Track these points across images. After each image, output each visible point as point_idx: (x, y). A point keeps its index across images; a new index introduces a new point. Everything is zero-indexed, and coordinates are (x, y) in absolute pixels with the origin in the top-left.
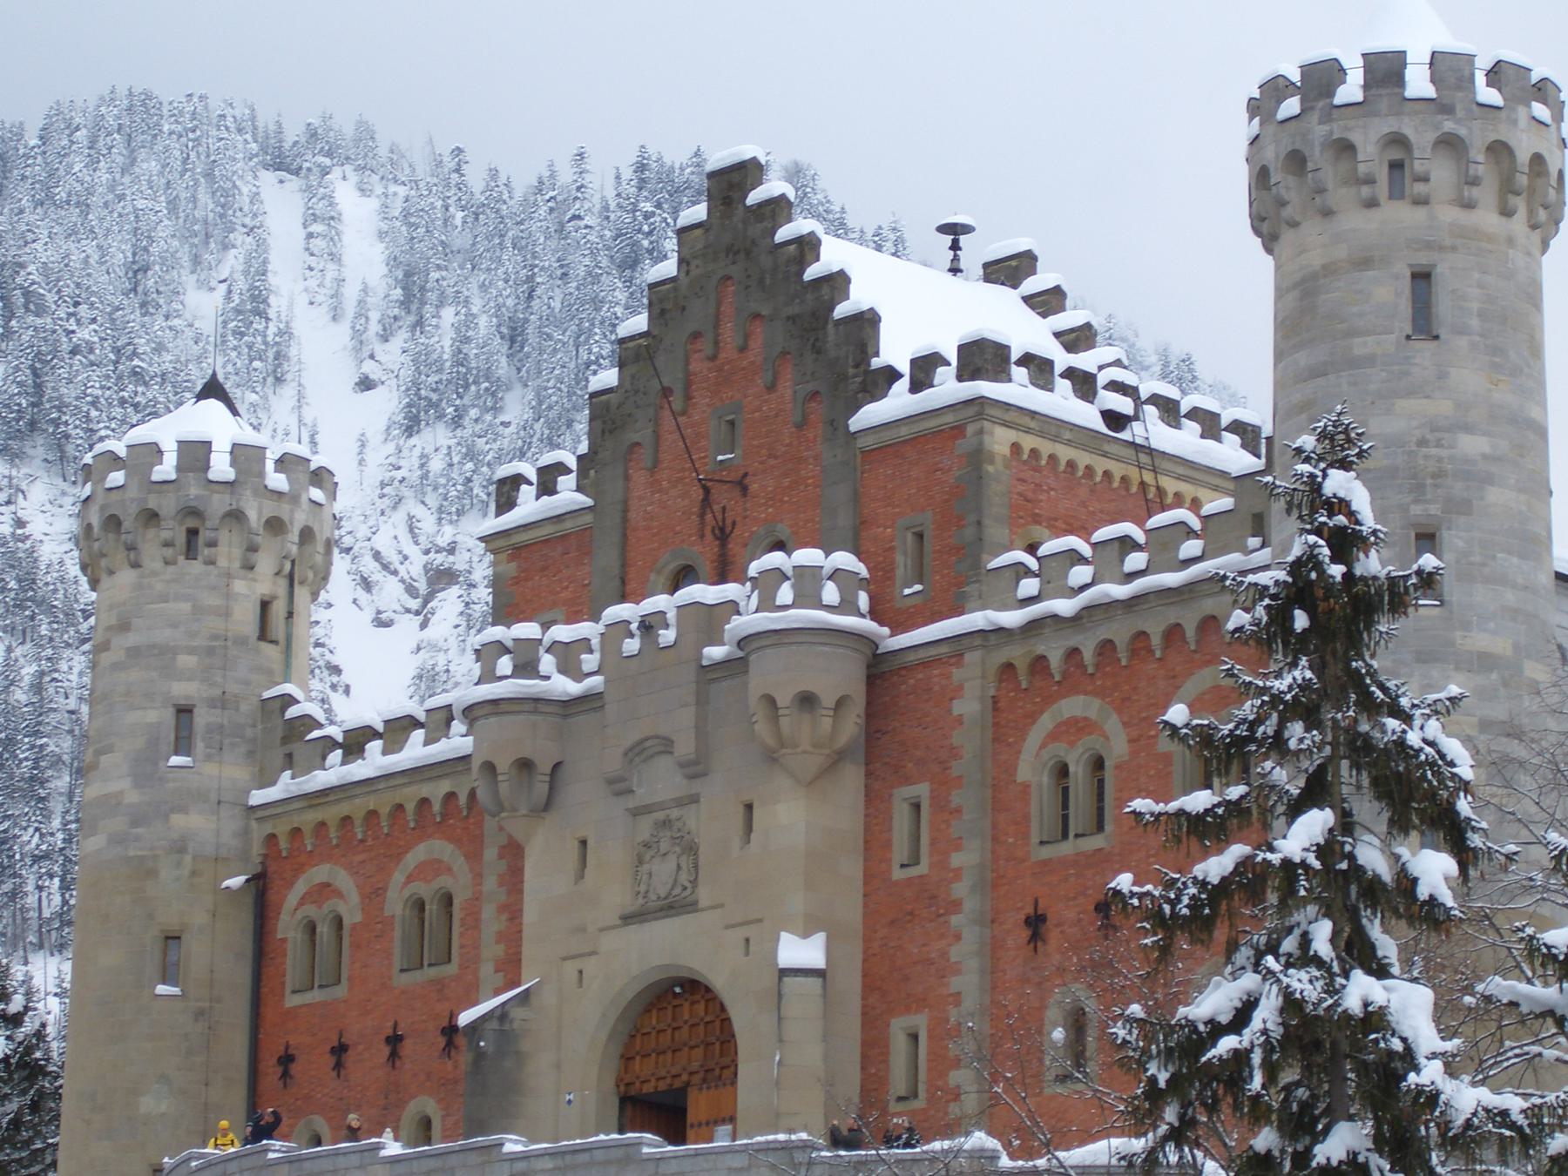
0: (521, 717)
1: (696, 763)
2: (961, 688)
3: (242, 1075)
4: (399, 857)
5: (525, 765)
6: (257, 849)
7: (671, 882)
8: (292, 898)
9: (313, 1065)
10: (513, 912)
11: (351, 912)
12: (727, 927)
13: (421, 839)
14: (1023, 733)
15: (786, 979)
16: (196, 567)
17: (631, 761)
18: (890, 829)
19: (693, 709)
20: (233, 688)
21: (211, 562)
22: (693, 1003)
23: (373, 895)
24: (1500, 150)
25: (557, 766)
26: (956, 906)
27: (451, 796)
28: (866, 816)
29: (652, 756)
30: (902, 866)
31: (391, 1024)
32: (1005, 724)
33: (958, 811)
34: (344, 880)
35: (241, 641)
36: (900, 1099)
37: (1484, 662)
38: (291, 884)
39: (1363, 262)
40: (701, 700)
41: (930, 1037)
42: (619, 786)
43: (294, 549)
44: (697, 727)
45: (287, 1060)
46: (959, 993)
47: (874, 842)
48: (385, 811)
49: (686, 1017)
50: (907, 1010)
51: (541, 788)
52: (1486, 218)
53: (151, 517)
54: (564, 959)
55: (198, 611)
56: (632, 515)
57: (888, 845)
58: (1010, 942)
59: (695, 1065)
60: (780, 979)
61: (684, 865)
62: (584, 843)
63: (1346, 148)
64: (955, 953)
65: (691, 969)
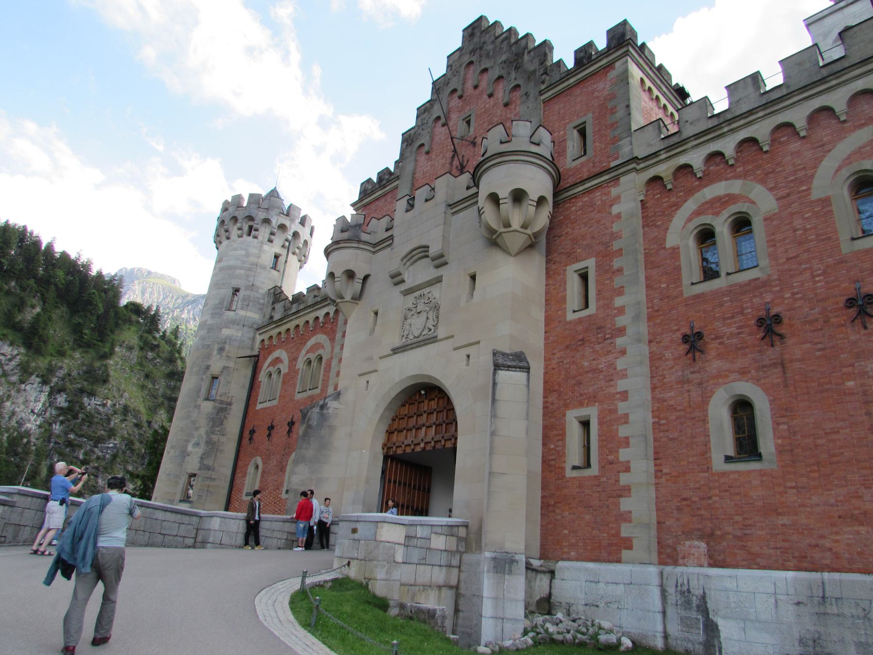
0: (350, 251)
1: (442, 256)
2: (619, 197)
3: (237, 437)
4: (305, 343)
5: (350, 275)
6: (257, 345)
7: (422, 327)
8: (266, 364)
9: (261, 435)
11: (284, 368)
12: (455, 349)
13: (314, 335)
14: (670, 217)
15: (500, 372)
16: (250, 239)
17: (405, 265)
18: (565, 290)
19: (442, 227)
20: (258, 284)
21: (255, 237)
22: (430, 400)
23: (293, 360)
25: (366, 278)
26: (622, 331)
27: (328, 314)
28: (547, 285)
29: (416, 261)
30: (574, 311)
31: (291, 416)
32: (654, 215)
33: (620, 270)
35: (264, 268)
36: (575, 468)
38: (266, 359)
41: (601, 423)
42: (397, 279)
43: (290, 238)
44: (443, 236)
45: (253, 432)
46: (626, 392)
47: (553, 300)
48: (301, 325)
49: (425, 409)
50: (581, 404)
51: (357, 285)
54: (360, 375)
56: (417, 175)
57: (564, 300)
58: (668, 354)
59: (428, 439)
60: (494, 374)
61: (431, 318)
62: (376, 313)
64: (620, 364)
65: (430, 377)
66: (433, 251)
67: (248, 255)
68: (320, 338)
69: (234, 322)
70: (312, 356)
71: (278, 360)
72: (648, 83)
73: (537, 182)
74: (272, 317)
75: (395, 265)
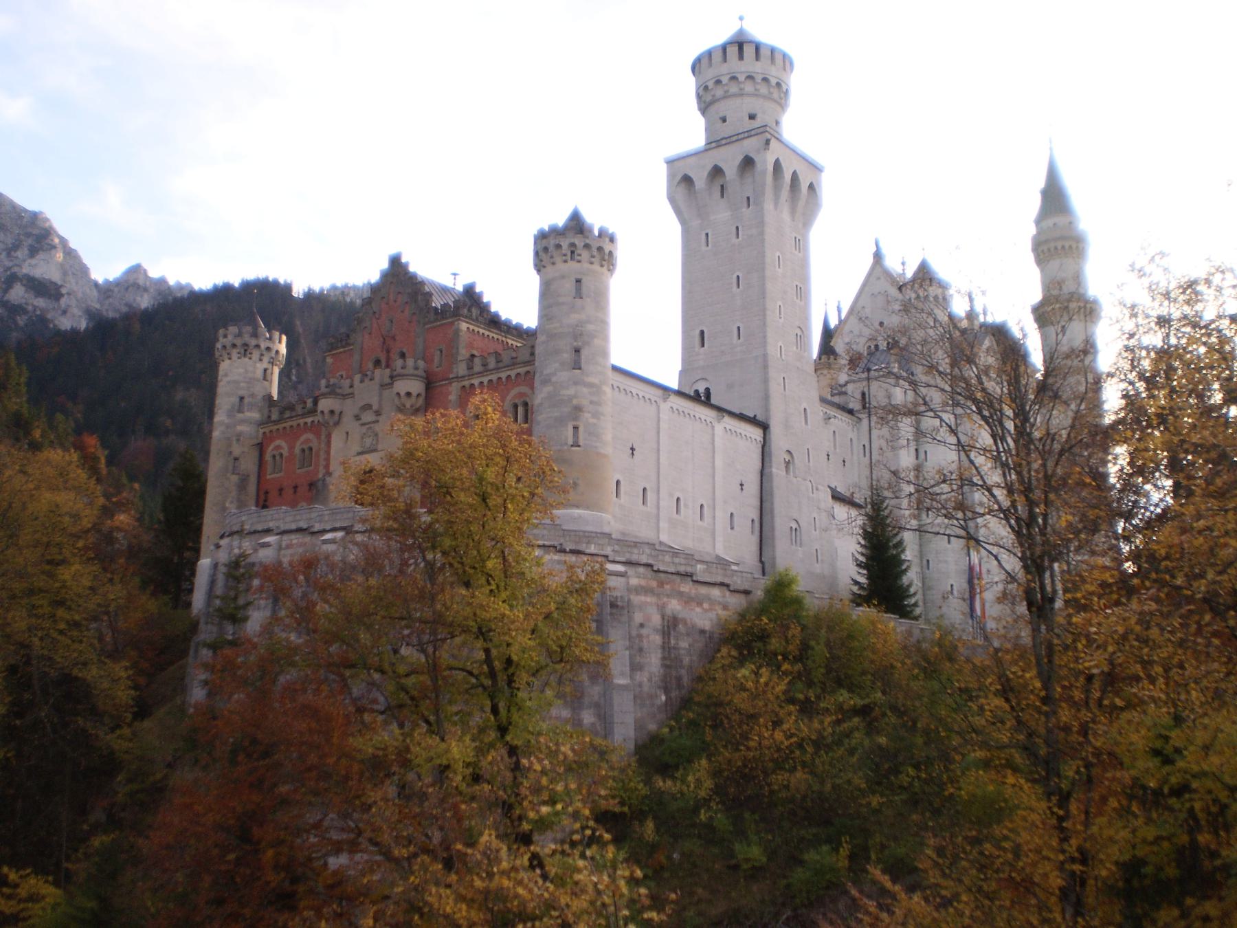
5: (332, 412)
6: (260, 435)
10: (328, 453)
11: (285, 452)
23: (291, 448)
24: (600, 249)
34: (283, 444)
37: (591, 385)
39: (563, 277)
40: (381, 395)
42: (357, 418)
45: (267, 493)
51: (336, 418)
52: (596, 267)
53: (234, 346)
55: (247, 371)
63: (559, 246)
66: (375, 407)
67: (247, 371)
68: (310, 436)
69: (242, 422)
70: (305, 447)
71: (278, 447)
72: (472, 327)
73: (416, 387)
74: (269, 417)
75: (356, 411)
